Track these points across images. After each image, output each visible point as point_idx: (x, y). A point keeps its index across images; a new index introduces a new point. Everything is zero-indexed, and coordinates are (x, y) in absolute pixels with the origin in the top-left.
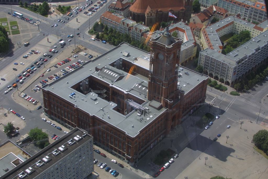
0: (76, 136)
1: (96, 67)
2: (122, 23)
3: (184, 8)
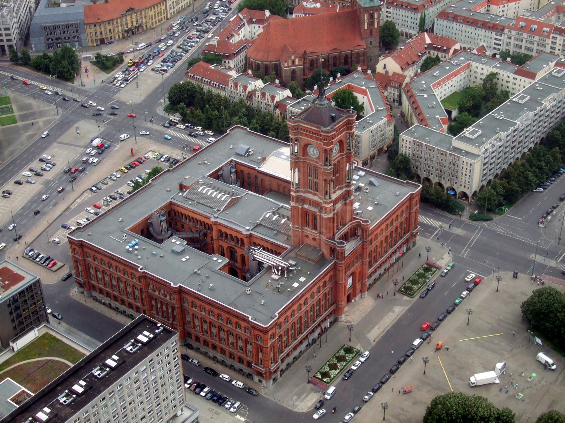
0: (141, 333)
1: (179, 182)
2: (232, 85)
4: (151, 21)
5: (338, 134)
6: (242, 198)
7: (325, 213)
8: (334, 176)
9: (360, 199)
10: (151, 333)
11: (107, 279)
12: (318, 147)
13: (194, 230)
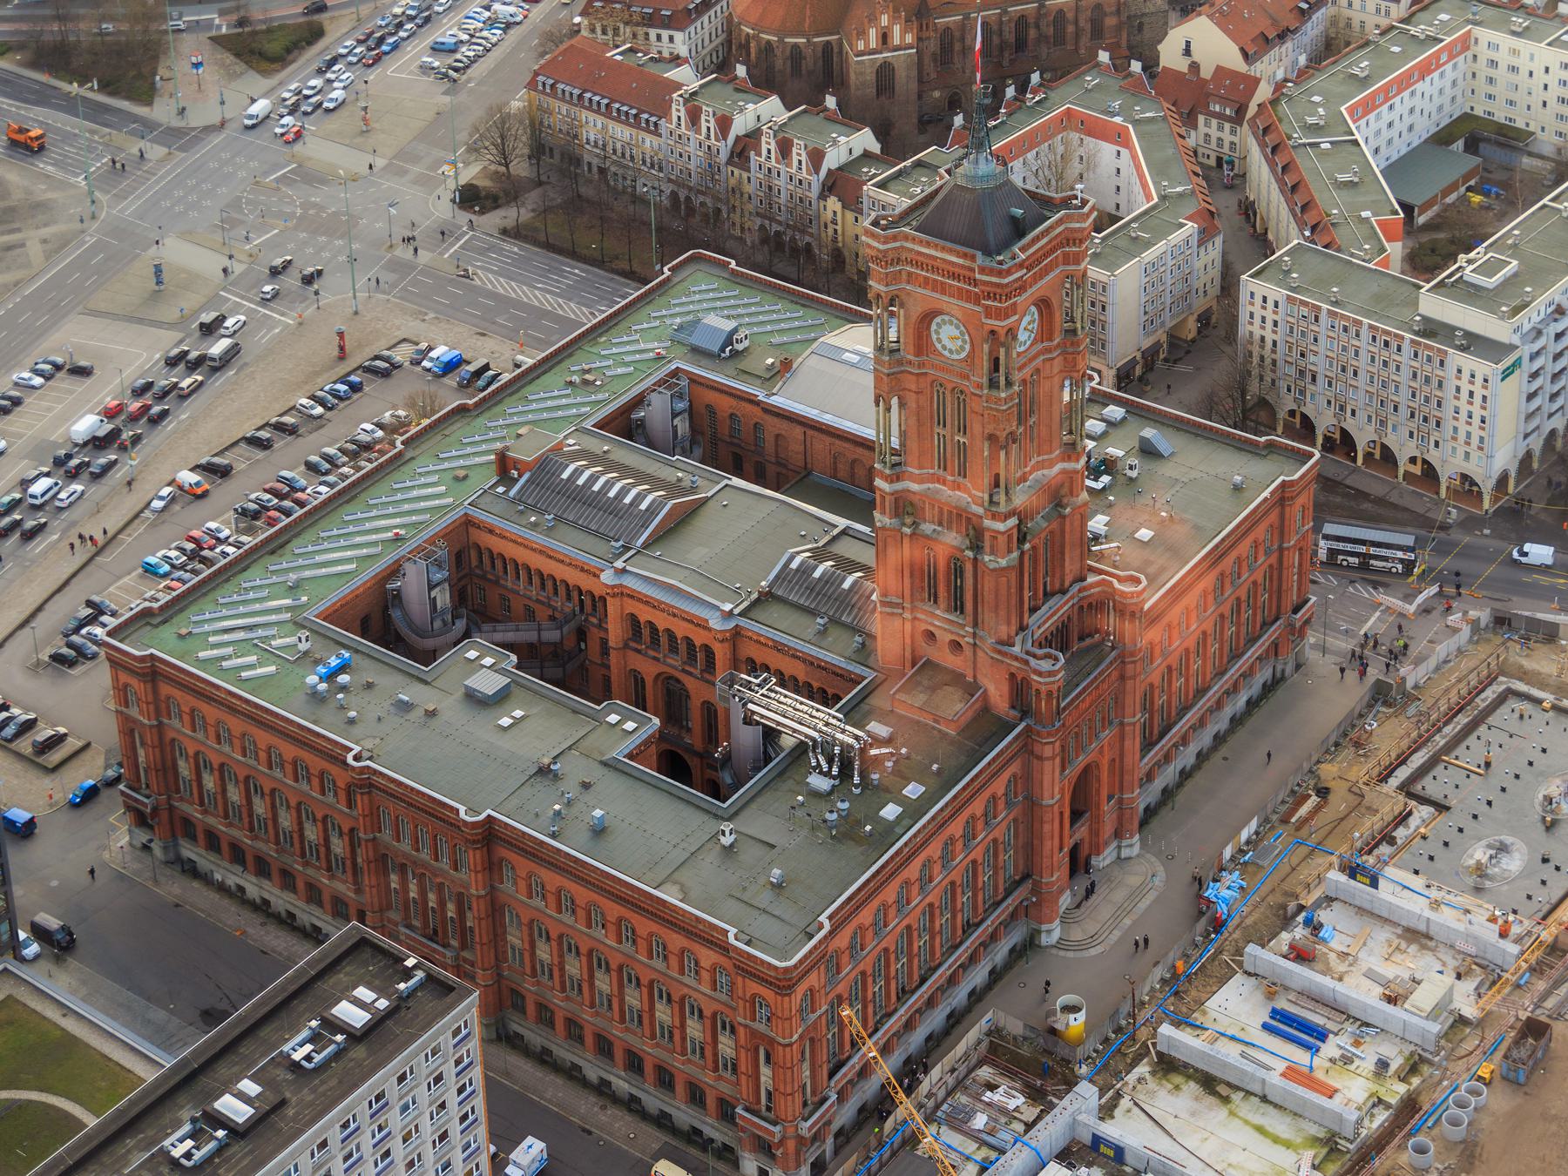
5: (1036, 279)
6: (710, 503)
7: (992, 553)
8: (1019, 424)
9: (1110, 505)
10: (381, 992)
11: (234, 794)
12: (967, 323)
13: (542, 613)
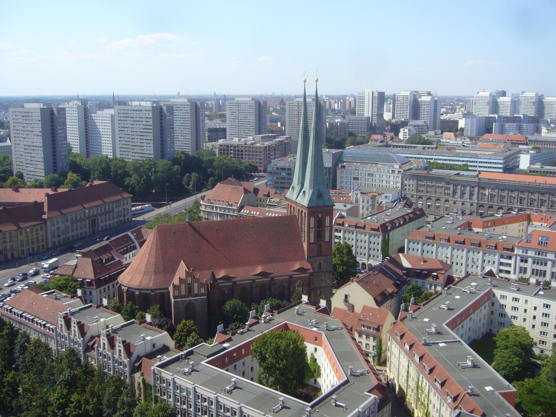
3: (308, 266)
4: (20, 249)
